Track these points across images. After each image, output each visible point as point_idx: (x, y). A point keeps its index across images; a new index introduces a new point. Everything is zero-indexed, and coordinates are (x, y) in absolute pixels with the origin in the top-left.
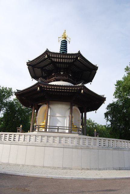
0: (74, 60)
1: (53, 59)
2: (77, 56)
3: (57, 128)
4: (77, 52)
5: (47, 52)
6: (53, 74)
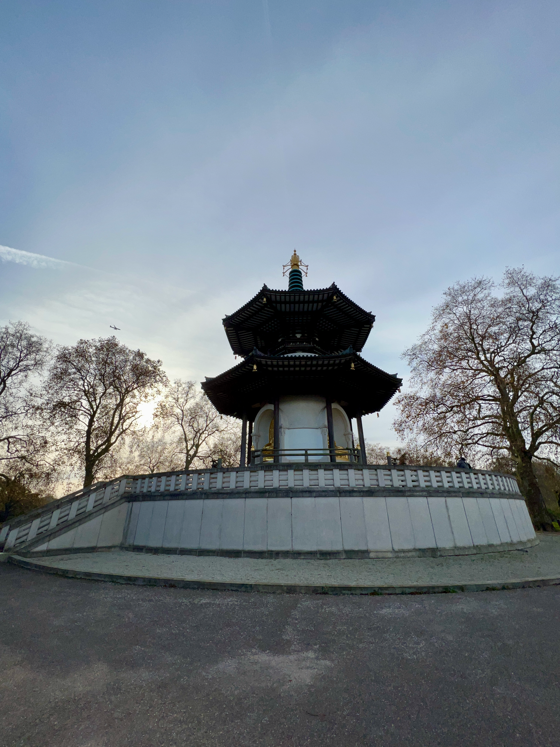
0: (324, 303)
1: (278, 305)
2: (330, 294)
3: (304, 452)
4: (328, 285)
5: (265, 291)
6: (280, 340)
